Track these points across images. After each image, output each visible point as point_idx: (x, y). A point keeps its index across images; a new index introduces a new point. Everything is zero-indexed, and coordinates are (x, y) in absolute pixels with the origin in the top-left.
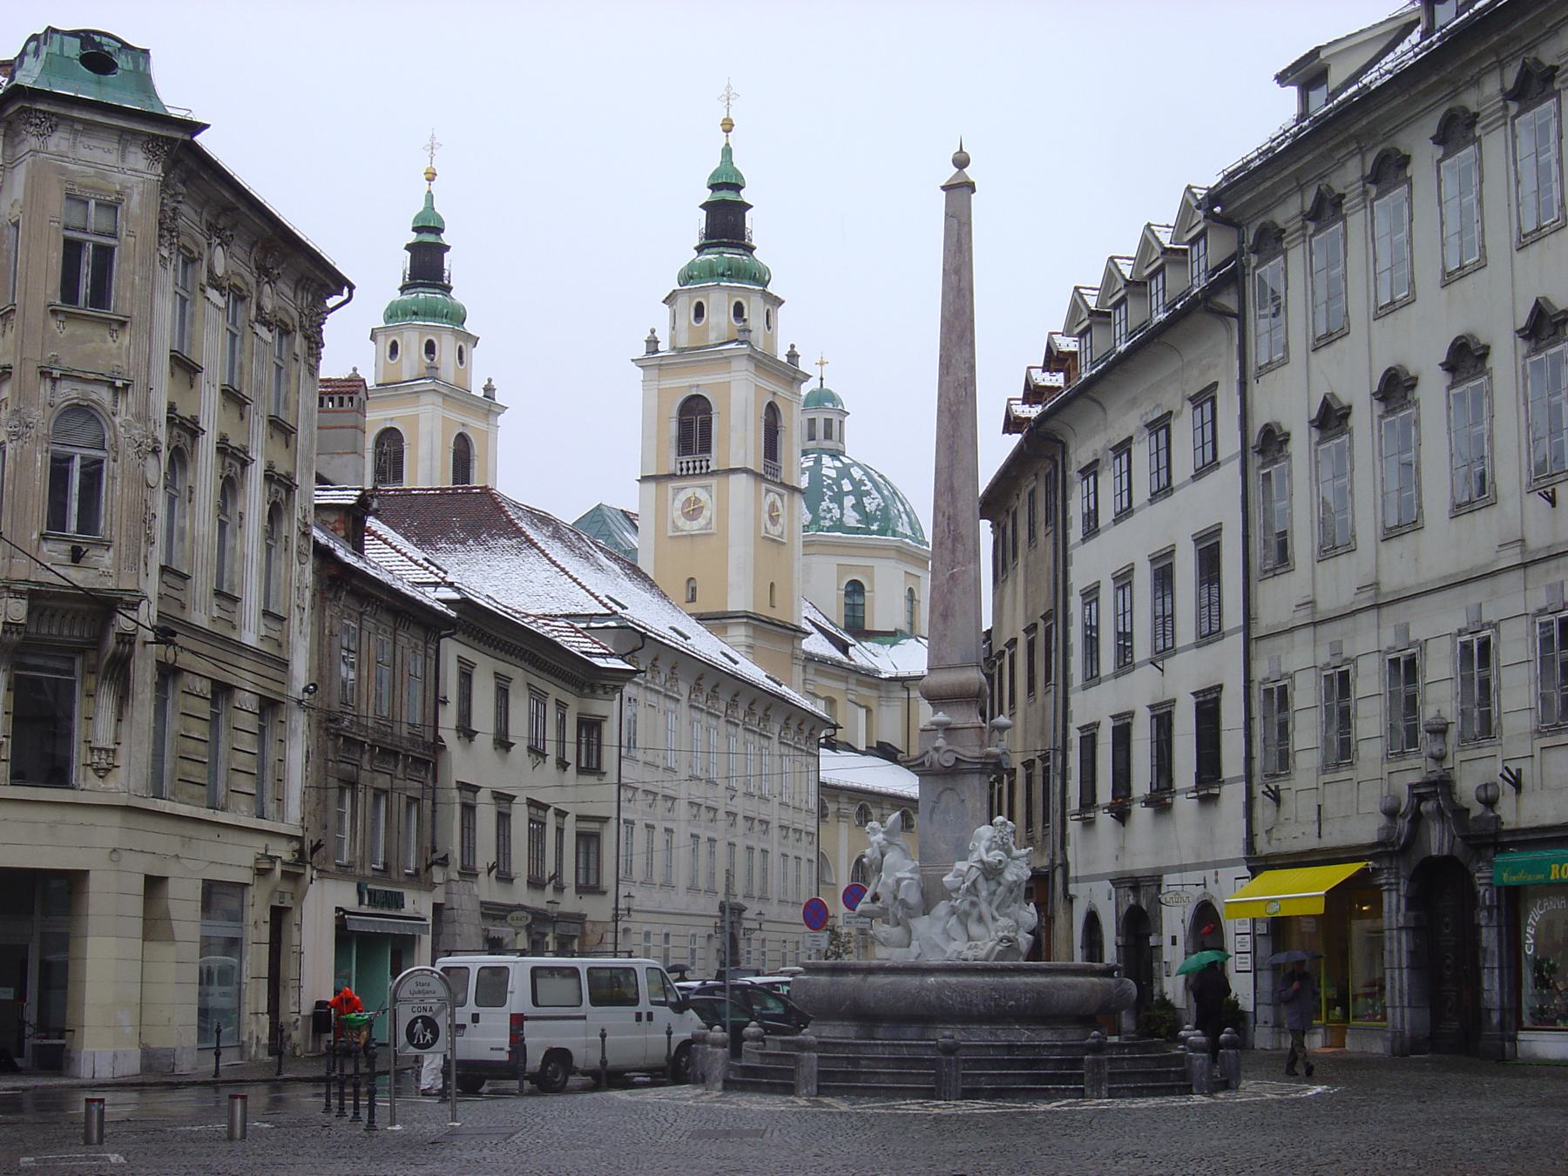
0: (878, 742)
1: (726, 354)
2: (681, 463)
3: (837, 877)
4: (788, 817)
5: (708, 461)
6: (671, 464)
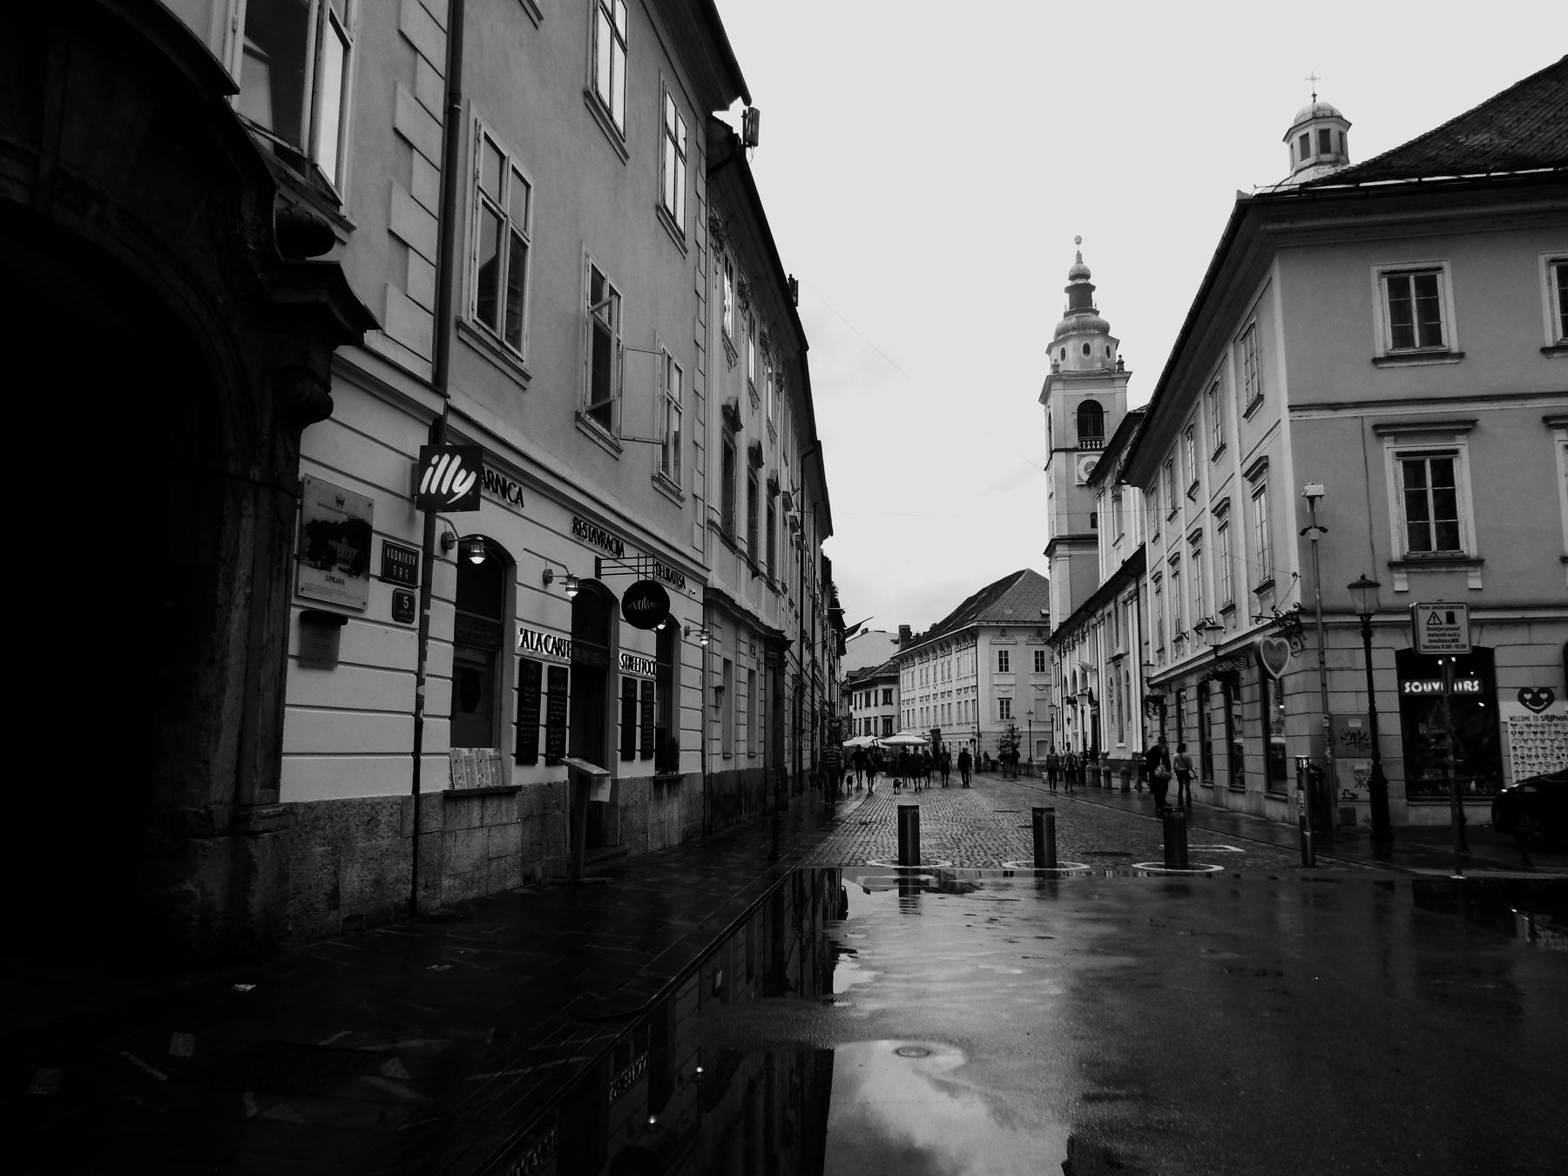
5: (1101, 441)
6: (1074, 441)
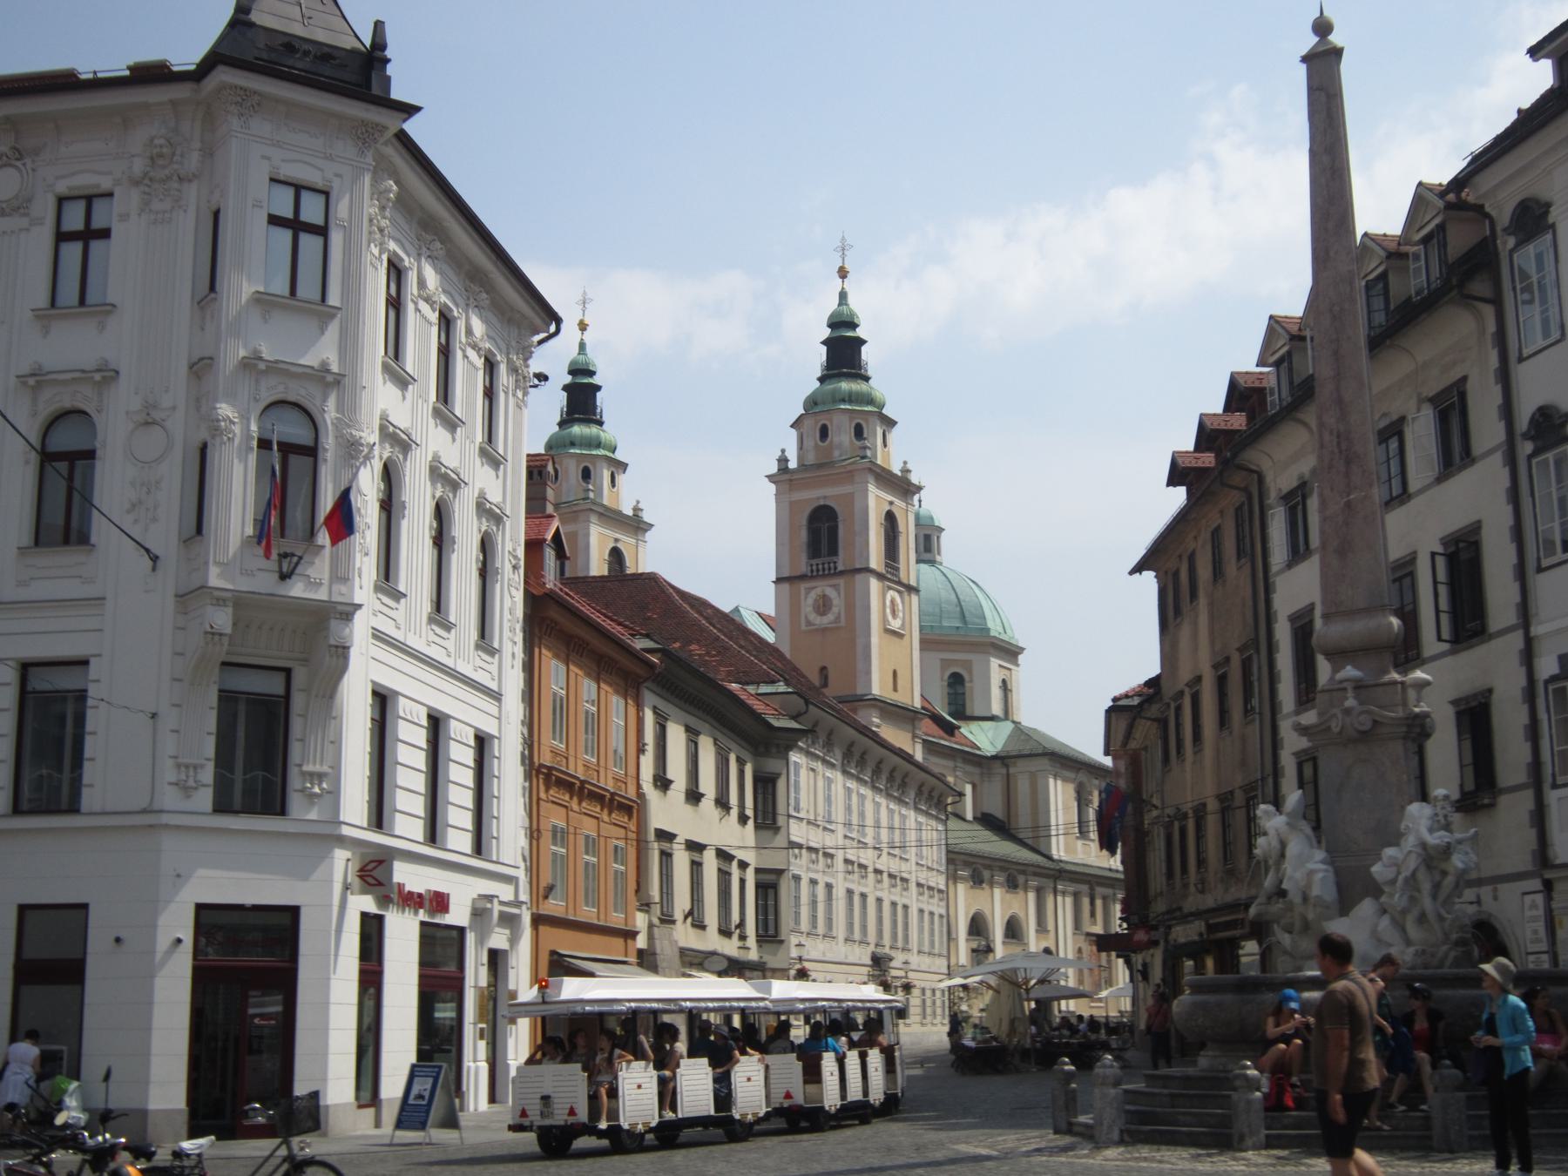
1: (849, 468)
2: (812, 565)
4: (923, 876)
5: (835, 563)
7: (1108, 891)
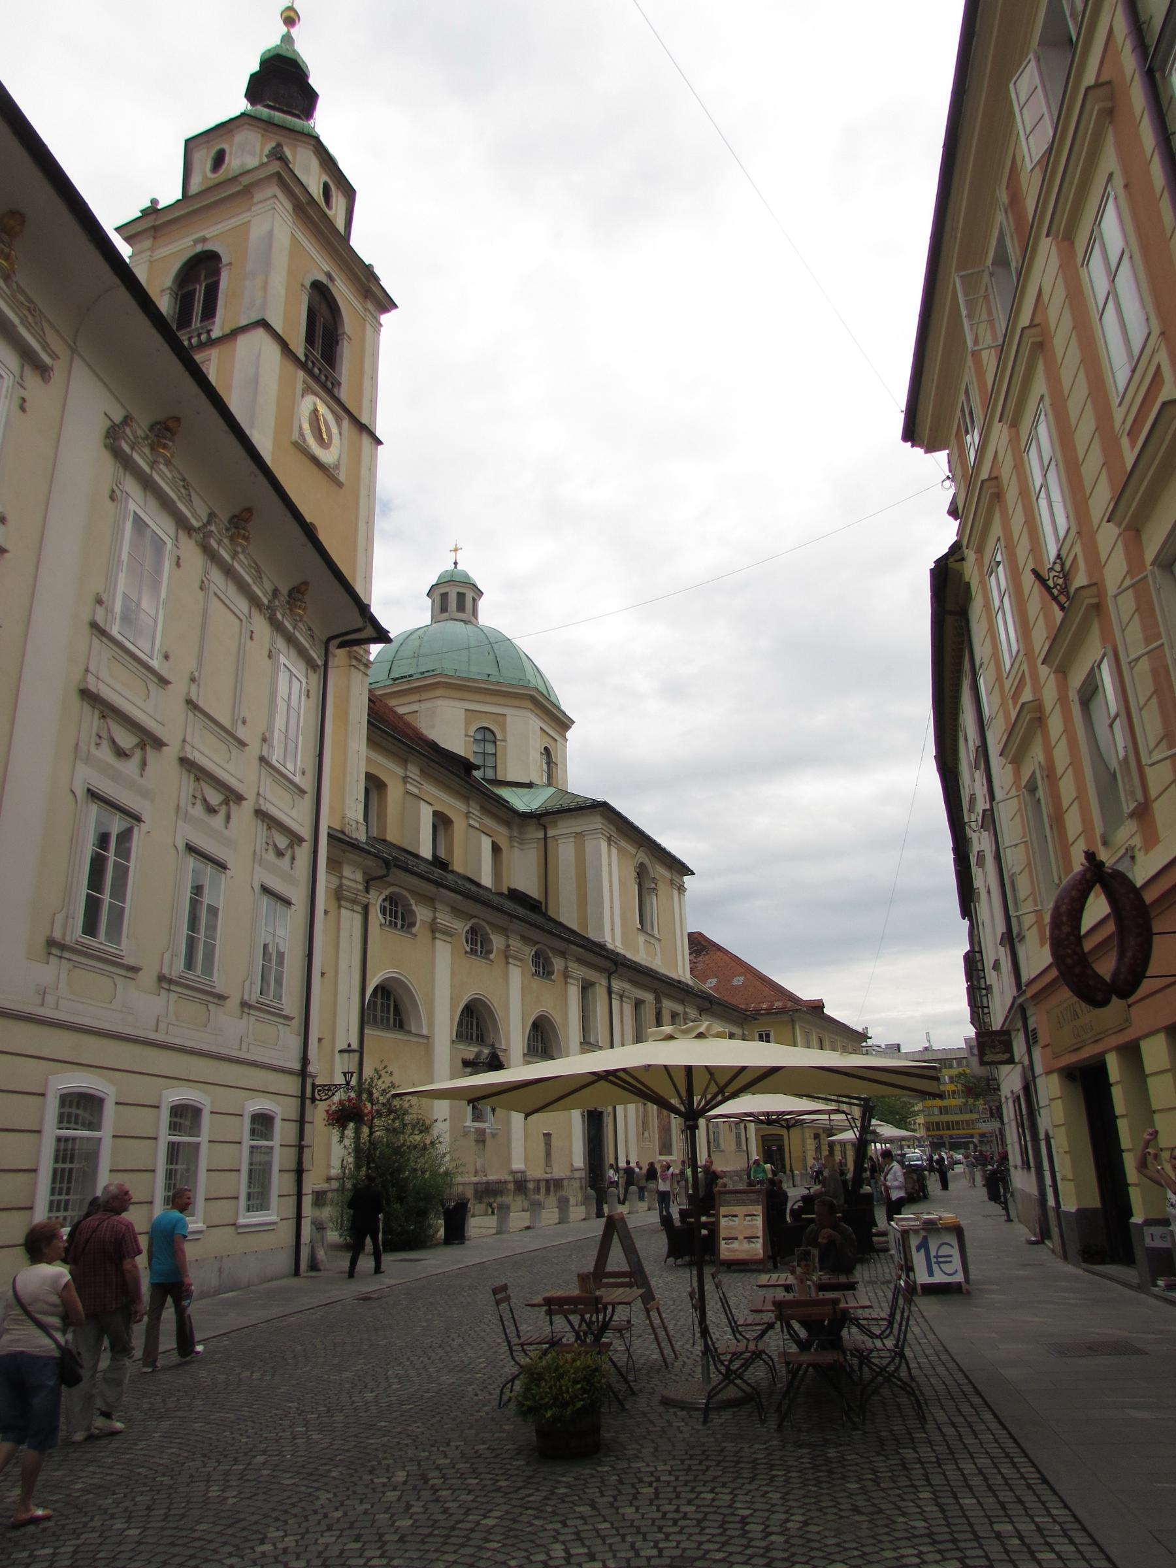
0: (509, 889)
3: (431, 1025)
7: (679, 1008)
